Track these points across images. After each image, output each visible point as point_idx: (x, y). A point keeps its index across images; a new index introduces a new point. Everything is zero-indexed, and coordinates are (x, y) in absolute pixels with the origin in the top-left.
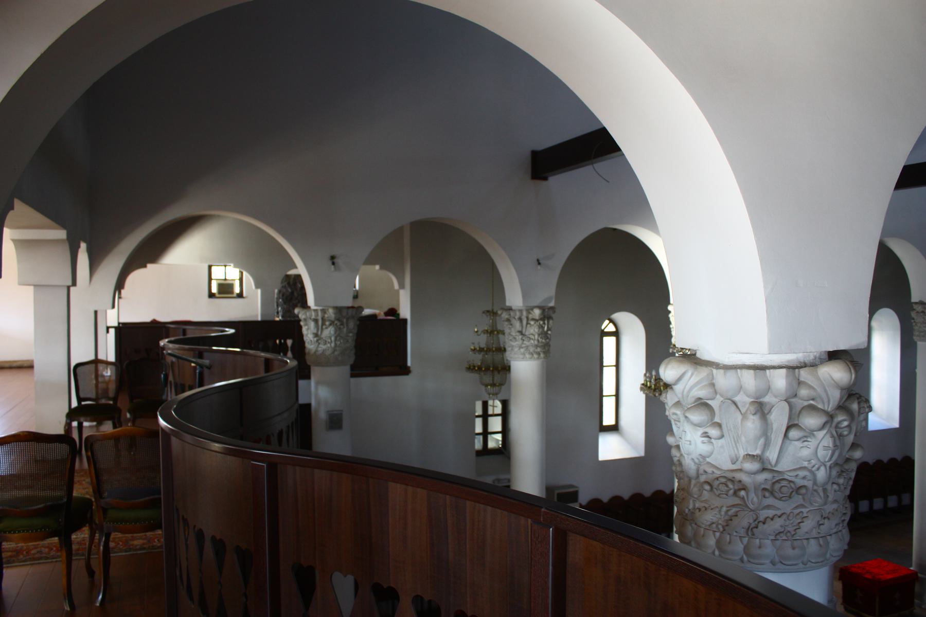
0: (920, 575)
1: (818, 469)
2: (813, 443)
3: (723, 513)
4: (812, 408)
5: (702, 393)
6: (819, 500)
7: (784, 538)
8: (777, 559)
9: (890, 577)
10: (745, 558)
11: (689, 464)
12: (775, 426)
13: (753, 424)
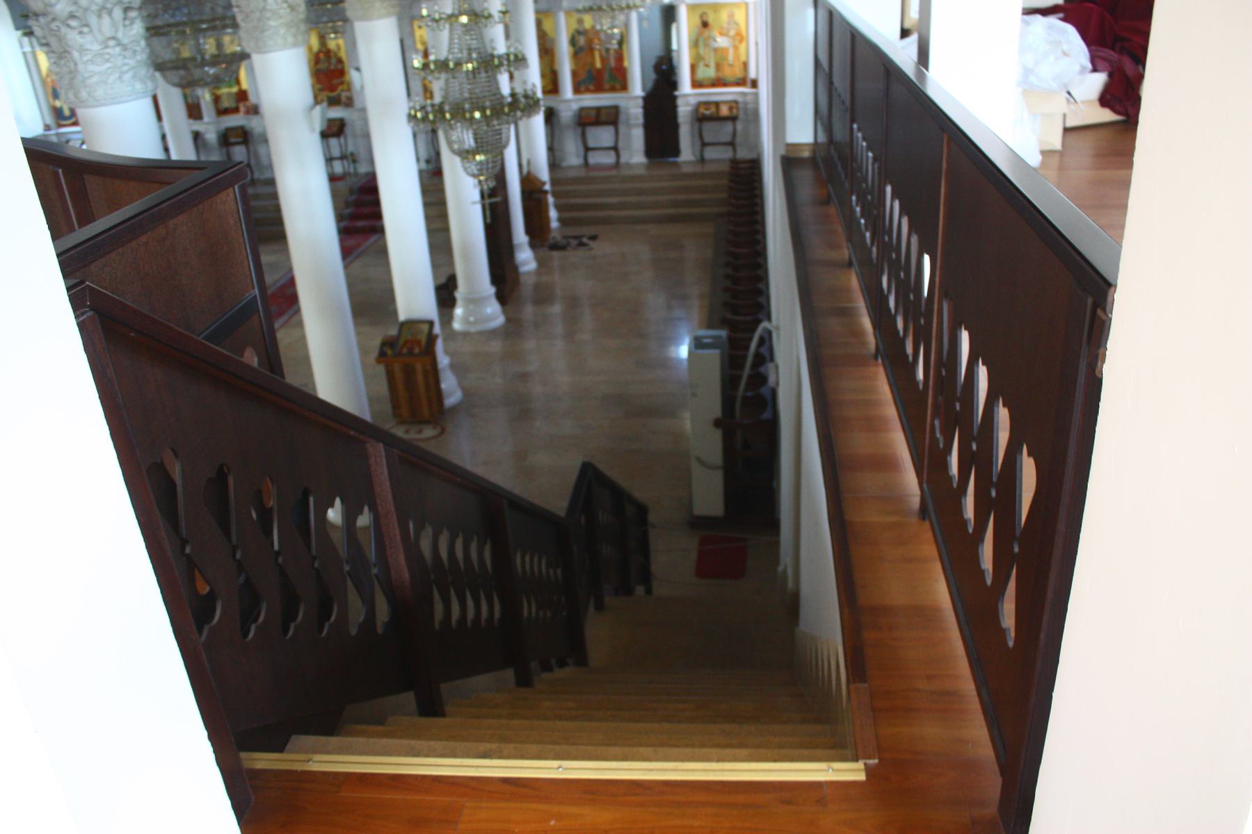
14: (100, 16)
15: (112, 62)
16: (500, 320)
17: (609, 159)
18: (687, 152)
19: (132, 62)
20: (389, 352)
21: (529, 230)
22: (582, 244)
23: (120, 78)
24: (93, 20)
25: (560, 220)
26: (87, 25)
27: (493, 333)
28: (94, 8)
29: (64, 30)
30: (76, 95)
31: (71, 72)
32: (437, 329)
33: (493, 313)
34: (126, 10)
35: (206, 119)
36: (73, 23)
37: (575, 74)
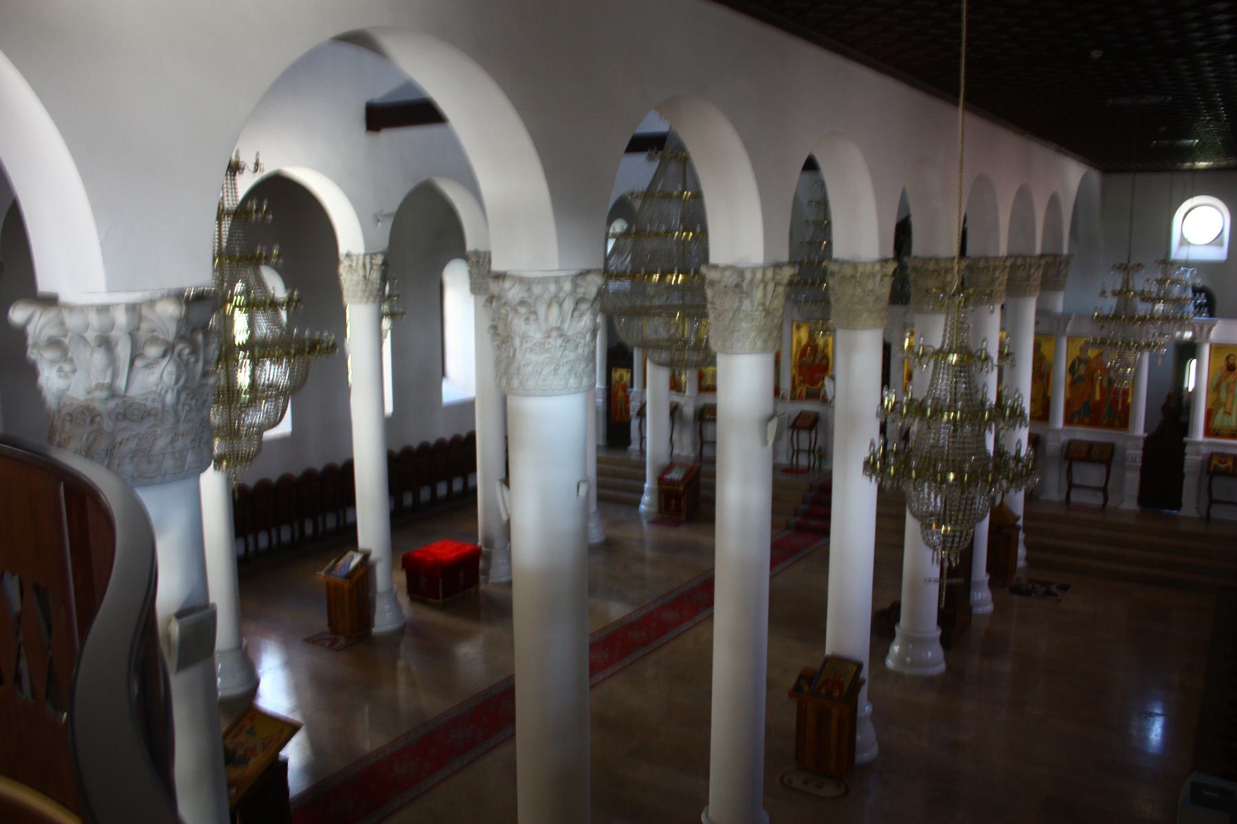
0: (483, 549)
1: (166, 392)
2: (157, 371)
3: (84, 439)
4: (154, 340)
5: (52, 331)
9: (454, 554)
11: (51, 400)
13: (99, 358)
15: (550, 352)
16: (942, 667)
17: (1095, 500)
18: (1190, 505)
20: (806, 688)
21: (990, 569)
22: (1048, 593)
23: (555, 370)
24: (542, 309)
25: (1027, 559)
26: (535, 313)
27: (929, 682)
28: (546, 296)
30: (508, 383)
31: (509, 357)
32: (865, 674)
33: (934, 658)
34: (578, 302)
35: (687, 393)
36: (523, 310)
37: (1068, 403)
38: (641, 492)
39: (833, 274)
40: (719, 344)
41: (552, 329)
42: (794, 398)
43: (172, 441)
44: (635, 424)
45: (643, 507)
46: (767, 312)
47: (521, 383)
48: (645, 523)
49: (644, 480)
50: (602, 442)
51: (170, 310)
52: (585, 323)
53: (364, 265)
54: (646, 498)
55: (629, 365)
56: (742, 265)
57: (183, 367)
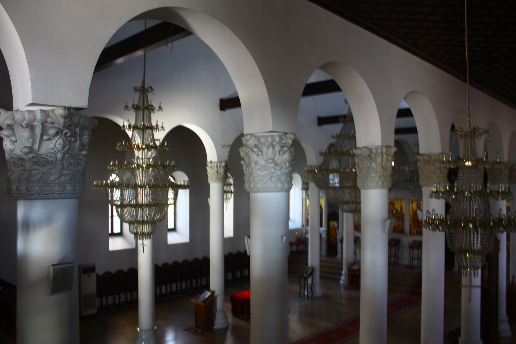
1: (58, 153)
2: (54, 142)
3: (18, 174)
5: (9, 122)
6: (59, 167)
7: (43, 182)
8: (39, 192)
10: (26, 193)
12: (38, 134)
13: (26, 133)
14: (268, 148)
19: (279, 173)
21: (508, 313)
23: (271, 179)
24: (265, 149)
26: (262, 152)
28: (267, 144)
29: (250, 152)
31: (250, 174)
34: (282, 147)
36: (255, 150)
38: (341, 275)
39: (420, 161)
40: (361, 184)
41: (269, 159)
42: (411, 234)
43: (59, 177)
44: (339, 245)
45: (341, 282)
46: (384, 168)
47: (255, 185)
48: (342, 290)
49: (342, 269)
50: (324, 253)
51: (60, 112)
52: (286, 158)
53: (217, 167)
54: (343, 278)
55: (337, 220)
56: (371, 146)
57: (68, 143)
